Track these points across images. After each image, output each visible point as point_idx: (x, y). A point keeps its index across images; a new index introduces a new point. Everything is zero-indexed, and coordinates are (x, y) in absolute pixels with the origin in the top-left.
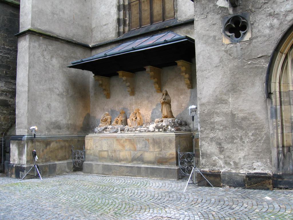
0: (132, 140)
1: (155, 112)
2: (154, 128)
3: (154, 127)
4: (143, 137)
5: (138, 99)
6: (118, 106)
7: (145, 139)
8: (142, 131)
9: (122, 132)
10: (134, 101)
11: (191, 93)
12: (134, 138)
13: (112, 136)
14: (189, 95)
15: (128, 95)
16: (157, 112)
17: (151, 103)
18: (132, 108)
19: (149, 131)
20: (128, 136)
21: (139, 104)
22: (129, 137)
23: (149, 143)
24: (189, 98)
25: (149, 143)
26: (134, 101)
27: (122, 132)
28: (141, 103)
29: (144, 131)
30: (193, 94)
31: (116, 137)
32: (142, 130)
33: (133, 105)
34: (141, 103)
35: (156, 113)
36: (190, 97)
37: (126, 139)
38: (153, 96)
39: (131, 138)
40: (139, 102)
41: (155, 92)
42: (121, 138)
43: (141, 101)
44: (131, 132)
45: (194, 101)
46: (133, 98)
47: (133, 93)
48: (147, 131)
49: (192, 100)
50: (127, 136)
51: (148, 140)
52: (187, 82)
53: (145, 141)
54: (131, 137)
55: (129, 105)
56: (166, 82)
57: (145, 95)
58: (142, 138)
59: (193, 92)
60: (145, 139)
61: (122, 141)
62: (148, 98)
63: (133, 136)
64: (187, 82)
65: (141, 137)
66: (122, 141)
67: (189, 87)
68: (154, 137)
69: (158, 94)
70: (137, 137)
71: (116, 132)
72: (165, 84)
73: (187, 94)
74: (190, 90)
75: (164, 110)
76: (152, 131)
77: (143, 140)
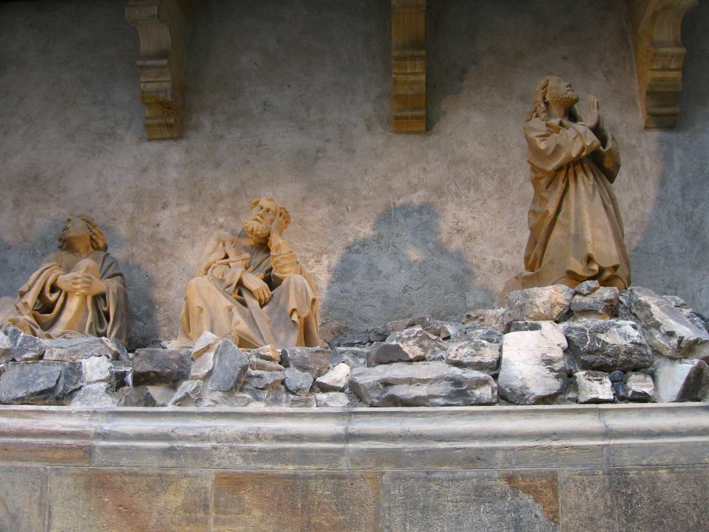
0: (322, 491)
1: (371, 266)
2: (549, 362)
3: (557, 353)
4: (474, 459)
5: (218, 165)
6: (17, 203)
7: (510, 479)
8: (422, 391)
9: (150, 401)
10: (173, 174)
11: (667, 159)
12: (344, 466)
13: (20, 433)
14: (651, 164)
15: (119, 132)
16: (385, 264)
17: (331, 201)
18: (147, 231)
19: (505, 397)
20: (258, 437)
21: (218, 199)
22: (278, 456)
23: (554, 517)
24: (651, 189)
25: (554, 517)
26: (173, 174)
27: (150, 401)
28: (236, 193)
29: (443, 388)
30: (677, 165)
31: (89, 452)
32: (410, 381)
33: (165, 206)
34: (236, 193)
35: (373, 272)
36: (663, 182)
37: (232, 483)
38: (351, 151)
39: (311, 469)
40: (223, 187)
41: (369, 128)
42: (152, 465)
43: (243, 183)
44: (276, 401)
45: (690, 208)
46: (174, 153)
47: (172, 118)
48: (485, 392)
49: (680, 200)
50: (245, 438)
51: (545, 487)
52: (659, 75)
53: (505, 506)
54: (304, 456)
55: (130, 208)
56: (464, 71)
57: (281, 139)
58: (460, 472)
59: (678, 153)
60: (510, 479)
61: (173, 500)
62: (304, 163)
63: (335, 438)
64: (659, 75)
65: (444, 458)
66: (173, 500)
67: (658, 111)
68: (627, 460)
69: (399, 139)
70: (396, 458)
71: (56, 395)
72: (462, 79)
73: (637, 161)
74: (655, 134)
75: (593, 226)
76: (540, 391)
77: (481, 493)
